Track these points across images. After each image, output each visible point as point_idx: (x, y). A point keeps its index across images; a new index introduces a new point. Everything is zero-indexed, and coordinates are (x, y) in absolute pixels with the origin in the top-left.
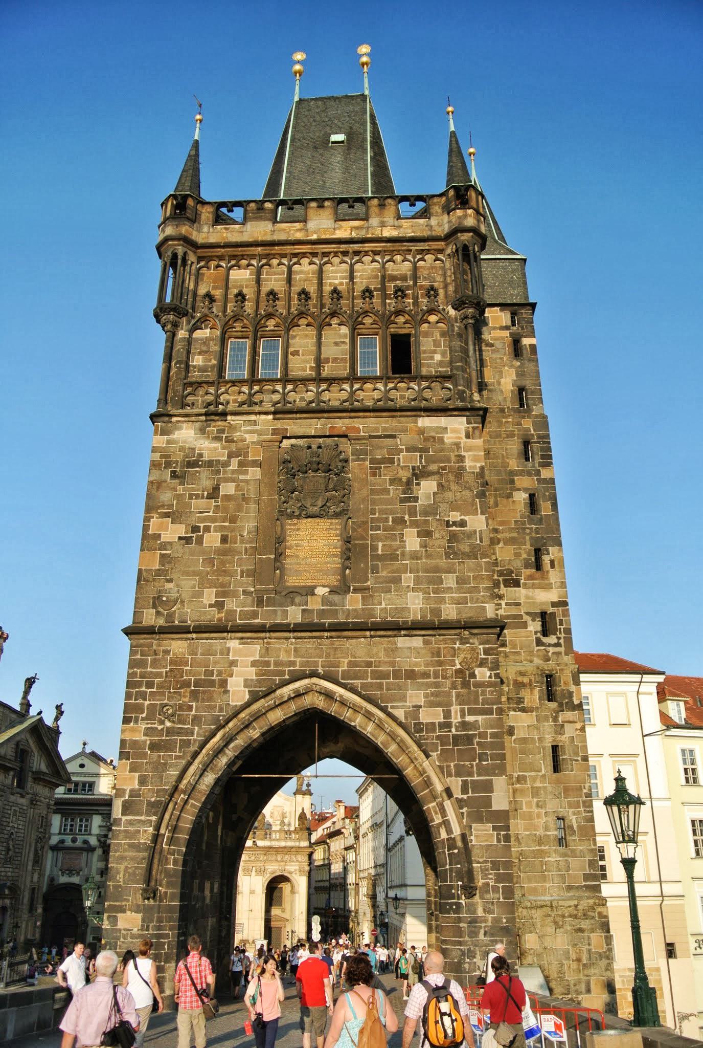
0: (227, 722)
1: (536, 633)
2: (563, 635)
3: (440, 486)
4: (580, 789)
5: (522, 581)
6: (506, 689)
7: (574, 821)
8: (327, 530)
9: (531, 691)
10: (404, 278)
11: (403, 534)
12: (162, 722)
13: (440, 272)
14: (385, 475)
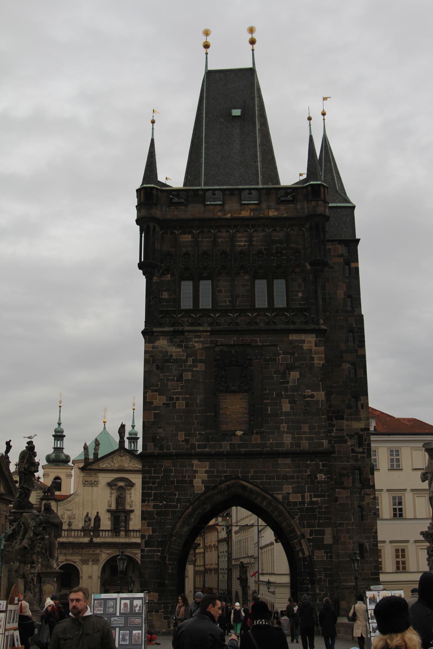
0: (195, 501)
1: (352, 446)
2: (366, 447)
3: (300, 374)
5: (345, 417)
6: (335, 477)
7: (368, 546)
8: (241, 399)
11: (281, 402)
12: (161, 502)
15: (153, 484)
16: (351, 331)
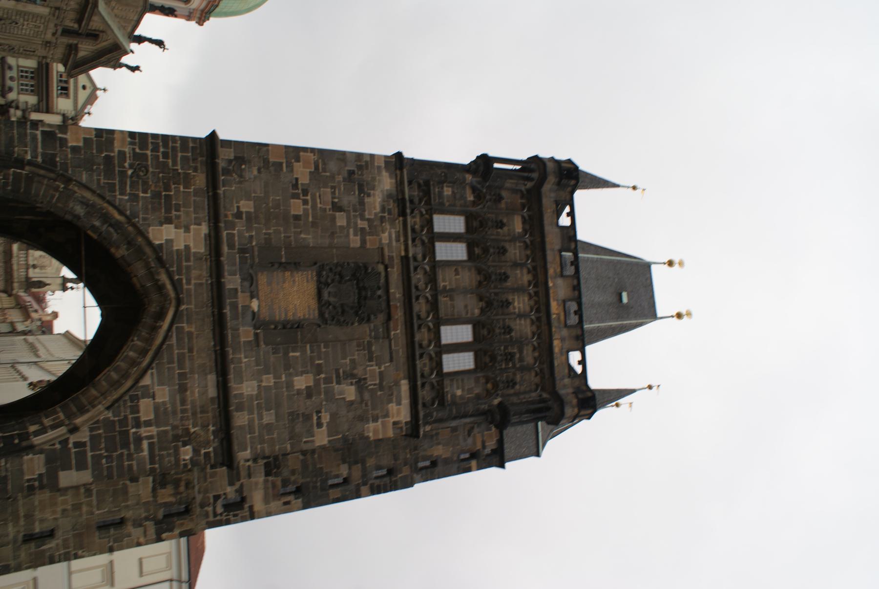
3: (352, 403)
4: (81, 547)
8: (309, 307)
9: (171, 495)
10: (521, 360)
13: (527, 389)
14: (358, 355)
15: (163, 153)
16: (390, 472)
